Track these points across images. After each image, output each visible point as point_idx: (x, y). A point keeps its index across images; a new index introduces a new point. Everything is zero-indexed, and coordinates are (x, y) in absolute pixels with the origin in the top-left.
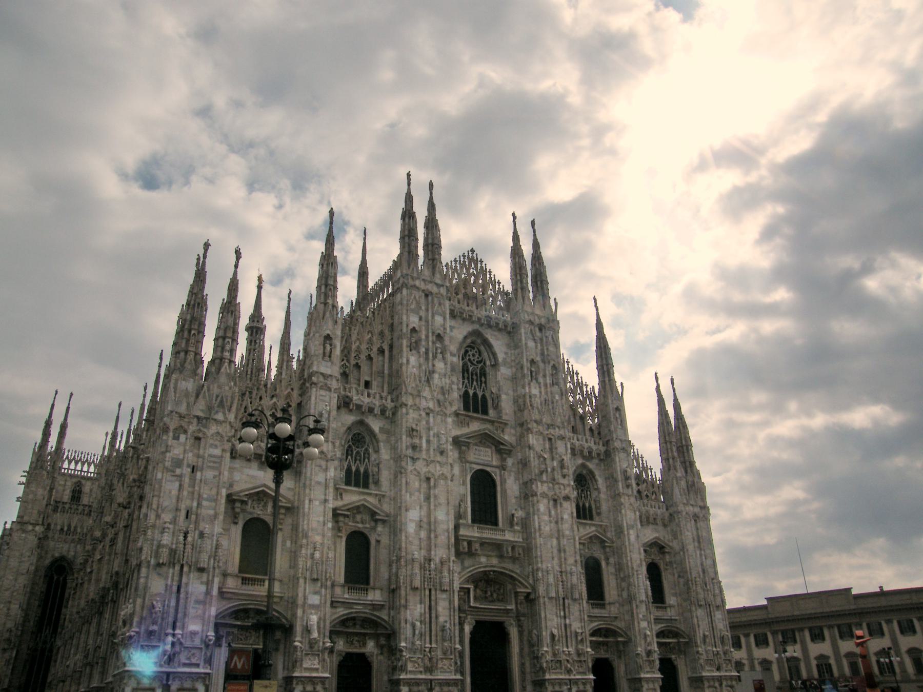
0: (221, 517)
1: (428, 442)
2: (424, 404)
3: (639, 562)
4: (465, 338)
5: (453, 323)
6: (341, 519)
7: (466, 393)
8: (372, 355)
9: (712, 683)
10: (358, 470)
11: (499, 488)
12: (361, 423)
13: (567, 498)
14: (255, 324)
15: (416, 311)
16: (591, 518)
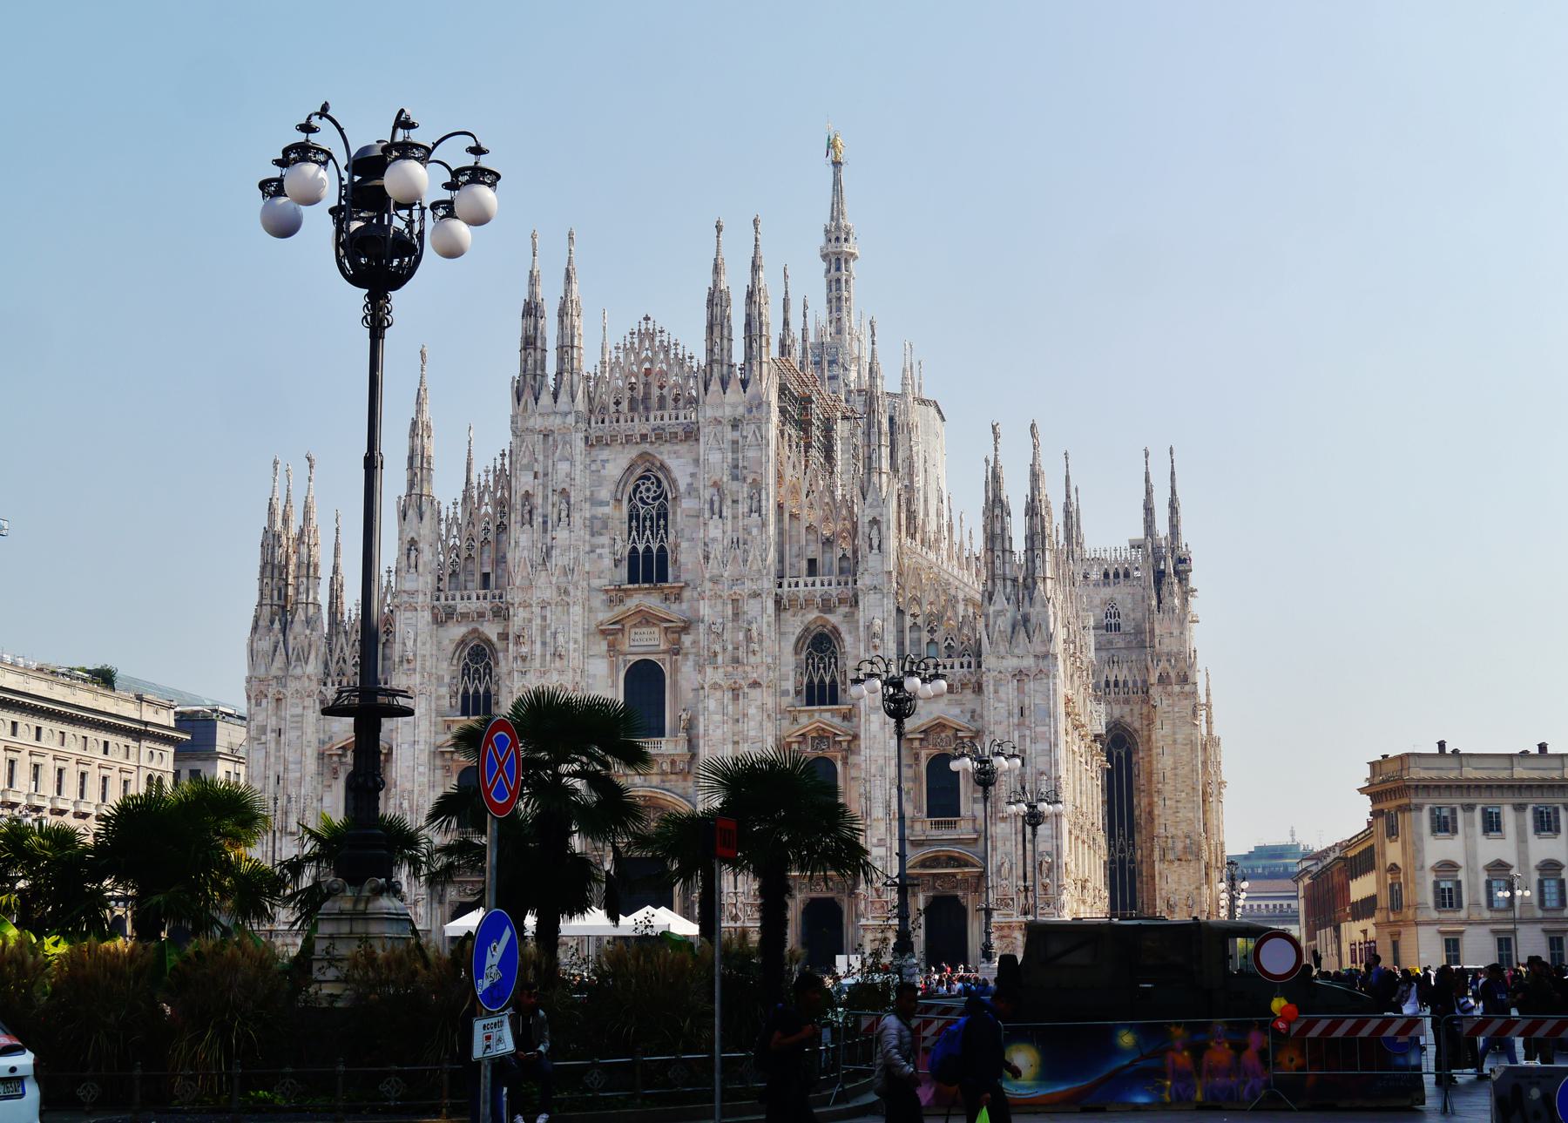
0: (308, 778)
1: (544, 644)
2: (537, 595)
3: (881, 762)
4: (630, 469)
5: (605, 454)
6: (448, 756)
7: (634, 550)
8: (490, 538)
9: (1006, 931)
10: (476, 691)
11: (668, 681)
12: (475, 630)
13: (755, 684)
14: (832, 248)
15: (528, 467)
16: (834, 701)
